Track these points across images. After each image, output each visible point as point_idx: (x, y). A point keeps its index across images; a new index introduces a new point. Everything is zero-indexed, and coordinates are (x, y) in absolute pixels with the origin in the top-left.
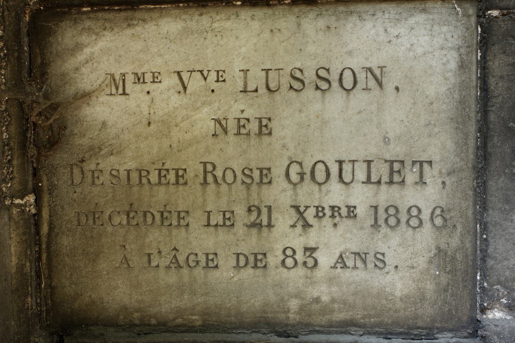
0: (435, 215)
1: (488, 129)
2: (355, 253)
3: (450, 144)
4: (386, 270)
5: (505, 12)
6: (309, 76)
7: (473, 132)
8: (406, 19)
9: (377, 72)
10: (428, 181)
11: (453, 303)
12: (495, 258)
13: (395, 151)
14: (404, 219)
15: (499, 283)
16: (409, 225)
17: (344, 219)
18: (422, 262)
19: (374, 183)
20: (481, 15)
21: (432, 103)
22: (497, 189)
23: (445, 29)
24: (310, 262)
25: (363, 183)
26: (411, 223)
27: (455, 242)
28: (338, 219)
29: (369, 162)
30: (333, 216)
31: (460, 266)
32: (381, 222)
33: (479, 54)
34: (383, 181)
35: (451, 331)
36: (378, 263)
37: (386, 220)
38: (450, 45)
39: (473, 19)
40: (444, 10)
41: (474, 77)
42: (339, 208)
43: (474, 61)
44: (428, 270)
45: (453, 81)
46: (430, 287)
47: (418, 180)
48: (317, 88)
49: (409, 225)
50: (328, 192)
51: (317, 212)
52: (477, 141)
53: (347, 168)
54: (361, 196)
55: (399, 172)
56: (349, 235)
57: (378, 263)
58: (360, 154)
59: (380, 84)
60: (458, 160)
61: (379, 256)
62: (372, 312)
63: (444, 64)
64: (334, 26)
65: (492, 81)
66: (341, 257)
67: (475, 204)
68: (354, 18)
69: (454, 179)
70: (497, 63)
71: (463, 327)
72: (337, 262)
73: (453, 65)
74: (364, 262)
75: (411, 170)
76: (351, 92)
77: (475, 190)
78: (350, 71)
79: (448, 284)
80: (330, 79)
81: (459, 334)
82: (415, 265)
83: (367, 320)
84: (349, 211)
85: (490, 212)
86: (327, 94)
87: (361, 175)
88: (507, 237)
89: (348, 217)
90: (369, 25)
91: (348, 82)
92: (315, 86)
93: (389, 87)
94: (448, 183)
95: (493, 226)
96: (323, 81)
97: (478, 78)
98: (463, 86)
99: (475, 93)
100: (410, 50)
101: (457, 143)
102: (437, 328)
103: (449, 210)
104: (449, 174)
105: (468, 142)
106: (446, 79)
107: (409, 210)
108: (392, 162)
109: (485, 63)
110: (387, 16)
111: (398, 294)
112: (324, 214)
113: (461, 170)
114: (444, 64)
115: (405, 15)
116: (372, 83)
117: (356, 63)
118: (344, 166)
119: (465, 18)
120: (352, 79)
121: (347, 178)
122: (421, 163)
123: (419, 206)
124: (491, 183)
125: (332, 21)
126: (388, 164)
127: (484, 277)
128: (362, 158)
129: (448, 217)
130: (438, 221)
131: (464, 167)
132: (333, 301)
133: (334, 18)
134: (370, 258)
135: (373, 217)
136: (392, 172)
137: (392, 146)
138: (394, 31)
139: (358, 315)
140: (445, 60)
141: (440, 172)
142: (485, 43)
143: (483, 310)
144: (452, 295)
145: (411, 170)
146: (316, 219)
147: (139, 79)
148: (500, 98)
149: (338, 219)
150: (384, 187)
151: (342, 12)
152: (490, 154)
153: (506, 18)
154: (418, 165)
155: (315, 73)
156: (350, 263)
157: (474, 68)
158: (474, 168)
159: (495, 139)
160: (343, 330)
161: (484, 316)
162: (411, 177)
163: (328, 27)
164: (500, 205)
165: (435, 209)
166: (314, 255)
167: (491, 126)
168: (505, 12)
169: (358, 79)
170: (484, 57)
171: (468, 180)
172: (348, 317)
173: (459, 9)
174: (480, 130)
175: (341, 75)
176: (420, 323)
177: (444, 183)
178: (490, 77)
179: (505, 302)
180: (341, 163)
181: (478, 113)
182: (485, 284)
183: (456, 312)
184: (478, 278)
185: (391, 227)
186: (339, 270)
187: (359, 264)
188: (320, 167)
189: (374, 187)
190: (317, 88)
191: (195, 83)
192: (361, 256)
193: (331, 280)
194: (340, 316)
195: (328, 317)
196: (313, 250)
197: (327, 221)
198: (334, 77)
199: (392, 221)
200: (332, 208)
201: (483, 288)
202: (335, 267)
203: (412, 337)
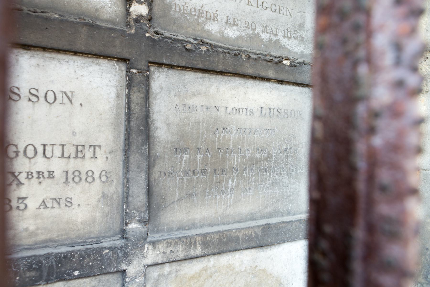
0: (102, 175)
1: (130, 129)
2: (53, 199)
3: (111, 137)
4: (72, 207)
5: (140, 71)
7: (123, 131)
8: (87, 67)
9: (70, 95)
10: (98, 157)
11: (111, 222)
12: (132, 197)
13: (79, 140)
14: (84, 177)
15: (135, 209)
16: (87, 182)
17: (46, 179)
18: (94, 201)
19: (66, 158)
20: (128, 71)
21: (101, 114)
22: (134, 161)
23: (109, 75)
24: (22, 206)
25: (59, 157)
26: (88, 180)
27: (112, 189)
28: (42, 179)
29: (63, 146)
30: (39, 178)
31: (115, 202)
32: (70, 180)
33: (127, 91)
34: (71, 156)
35: (109, 237)
36: (68, 204)
37: (73, 179)
38: (112, 84)
39: (124, 73)
40: (109, 66)
41: (124, 103)
42: (43, 173)
43: (125, 94)
44: (97, 205)
45: (113, 103)
46: (98, 214)
47: (92, 156)
48: (30, 100)
49: (87, 182)
50: (35, 163)
51: (28, 175)
52: (125, 136)
53: (49, 149)
54: (57, 166)
55: (82, 151)
56: (49, 189)
57: (68, 204)
58: (58, 141)
59: (71, 101)
60: (115, 145)
61: (68, 199)
62: (64, 233)
63: (108, 94)
64: (42, 65)
65: (132, 106)
66: (44, 201)
67: (124, 169)
68: (55, 62)
69: (112, 156)
70: (135, 96)
71: (116, 234)
72: (41, 205)
73: (113, 95)
74: (59, 204)
75: (89, 150)
76: (52, 104)
77: (124, 161)
78: (52, 92)
79: (109, 212)
80: (39, 95)
81: (114, 238)
82: (90, 203)
83: (60, 237)
84: (49, 175)
85: (131, 172)
86: (36, 104)
87: (58, 152)
88: (139, 185)
89: (49, 177)
90: (65, 67)
91: (51, 98)
92: (28, 99)
93: (76, 103)
94: (109, 157)
95: (132, 180)
97: (126, 103)
98: (118, 106)
99: (123, 111)
100: (89, 84)
101: (114, 137)
102: (102, 237)
103: (110, 172)
104: (110, 153)
105: (121, 136)
106: (109, 102)
107: (87, 173)
108: (77, 146)
109: (130, 95)
110: (76, 63)
111: (80, 220)
112: (33, 177)
113: (116, 151)
114: (108, 94)
115: (86, 65)
116: (66, 100)
117: (56, 88)
118: (47, 148)
119: (120, 71)
120: (53, 97)
121: (48, 154)
122: (95, 147)
123: (93, 170)
124: (132, 159)
125: (41, 61)
126: (75, 147)
127: (127, 206)
128: (59, 143)
129: (109, 176)
130: (104, 178)
131: (118, 149)
132: (38, 229)
133: (42, 60)
134: (63, 202)
135: (65, 177)
136: (77, 151)
137: (77, 137)
138: (80, 73)
139: (54, 235)
140: (109, 92)
141: (105, 152)
142: (129, 86)
143: (127, 224)
144: (111, 218)
145: (89, 150)
146: (27, 180)
148: (137, 114)
149: (42, 179)
150: (72, 160)
151: (48, 57)
152: (131, 142)
153: (140, 74)
154: (92, 148)
155: (28, 91)
156: (49, 205)
157: (124, 98)
158: (123, 150)
159: (134, 135)
160: (44, 245)
161: (127, 227)
162: (88, 154)
163: (38, 65)
164: (135, 169)
165: (101, 172)
166: (25, 202)
167: (132, 128)
168: (140, 71)
169: (57, 97)
170: (129, 92)
171: (120, 157)
172: (48, 237)
173: (117, 66)
174: (126, 130)
175: (46, 94)
176: (92, 235)
177: (107, 158)
178: (132, 103)
179: (138, 218)
180: (44, 146)
181: (126, 121)
182: (128, 210)
183: (113, 227)
184: (125, 207)
185: (76, 183)
186: (42, 210)
187: (56, 205)
188: (30, 148)
189: (66, 160)
190: (30, 100)
192: (57, 200)
193: (36, 217)
194: (41, 237)
195: (34, 239)
196: (25, 198)
197: (34, 181)
198: (41, 95)
199: (77, 179)
200: (38, 172)
201: (126, 212)
202: (39, 208)
203: (88, 243)
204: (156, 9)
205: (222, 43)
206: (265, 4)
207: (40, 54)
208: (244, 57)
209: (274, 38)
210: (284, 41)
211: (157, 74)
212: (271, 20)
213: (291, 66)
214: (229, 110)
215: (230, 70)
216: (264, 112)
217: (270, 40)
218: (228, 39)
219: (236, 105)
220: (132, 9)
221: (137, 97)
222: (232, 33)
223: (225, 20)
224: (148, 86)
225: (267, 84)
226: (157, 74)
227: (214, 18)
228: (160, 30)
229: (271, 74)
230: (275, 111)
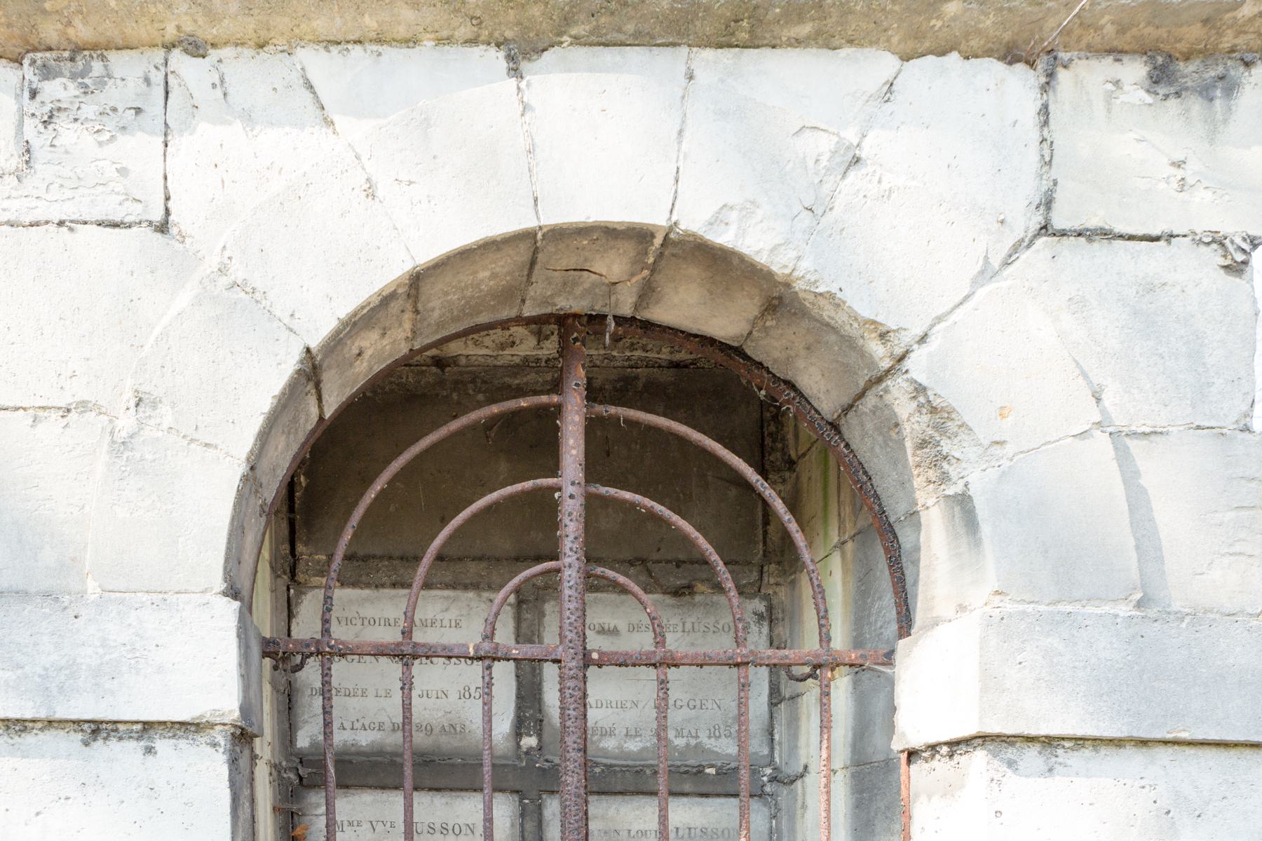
6: (437, 827)
73: (508, 825)
90: (467, 803)
91: (457, 831)
96: (444, 829)
117: (461, 821)
125: (449, 800)
142: (522, 815)
147: (350, 824)
191: (379, 828)
198: (450, 828)
204: (545, 736)
205: (621, 759)
206: (679, 703)
207: (448, 793)
208: (648, 772)
209: (693, 742)
210: (709, 743)
211: (549, 801)
212: (689, 720)
213: (718, 774)
214: (633, 833)
215: (632, 789)
216: (681, 833)
217: (688, 745)
218: (629, 755)
219: (642, 827)
220: (522, 743)
221: (530, 826)
222: (633, 746)
223: (624, 732)
224: (541, 814)
225: (685, 800)
226: (549, 801)
227: (610, 733)
228: (550, 757)
229: (687, 788)
230: (698, 831)
